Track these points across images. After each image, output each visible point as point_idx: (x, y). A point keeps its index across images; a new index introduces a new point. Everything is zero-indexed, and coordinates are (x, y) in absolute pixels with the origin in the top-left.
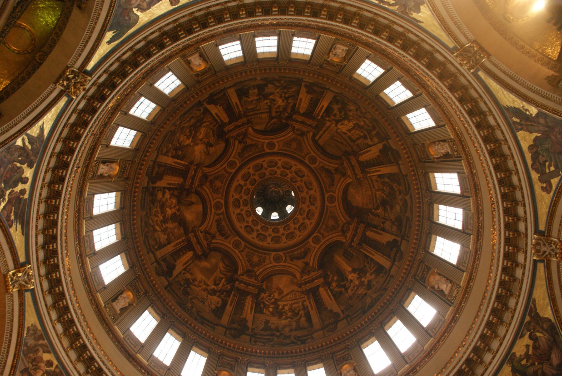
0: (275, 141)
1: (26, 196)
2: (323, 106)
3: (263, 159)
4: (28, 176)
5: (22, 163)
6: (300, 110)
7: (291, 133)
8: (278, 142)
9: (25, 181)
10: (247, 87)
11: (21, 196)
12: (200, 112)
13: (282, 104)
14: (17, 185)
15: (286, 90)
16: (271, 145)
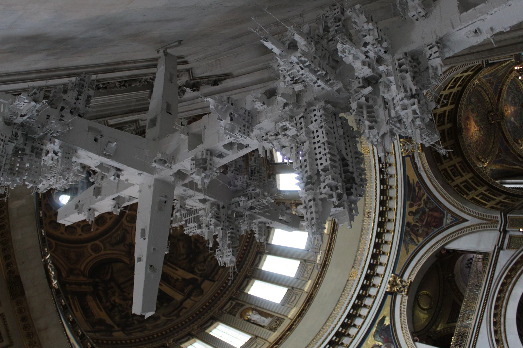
0: (94, 255)
1: (408, 203)
2: (77, 311)
3: (98, 231)
4: (410, 217)
5: (415, 226)
6: (92, 298)
7: (82, 268)
8: (91, 255)
9: (411, 213)
10: (165, 305)
11: (412, 202)
12: (198, 269)
13: (113, 298)
14: (416, 210)
15: (123, 314)
16: (96, 249)
